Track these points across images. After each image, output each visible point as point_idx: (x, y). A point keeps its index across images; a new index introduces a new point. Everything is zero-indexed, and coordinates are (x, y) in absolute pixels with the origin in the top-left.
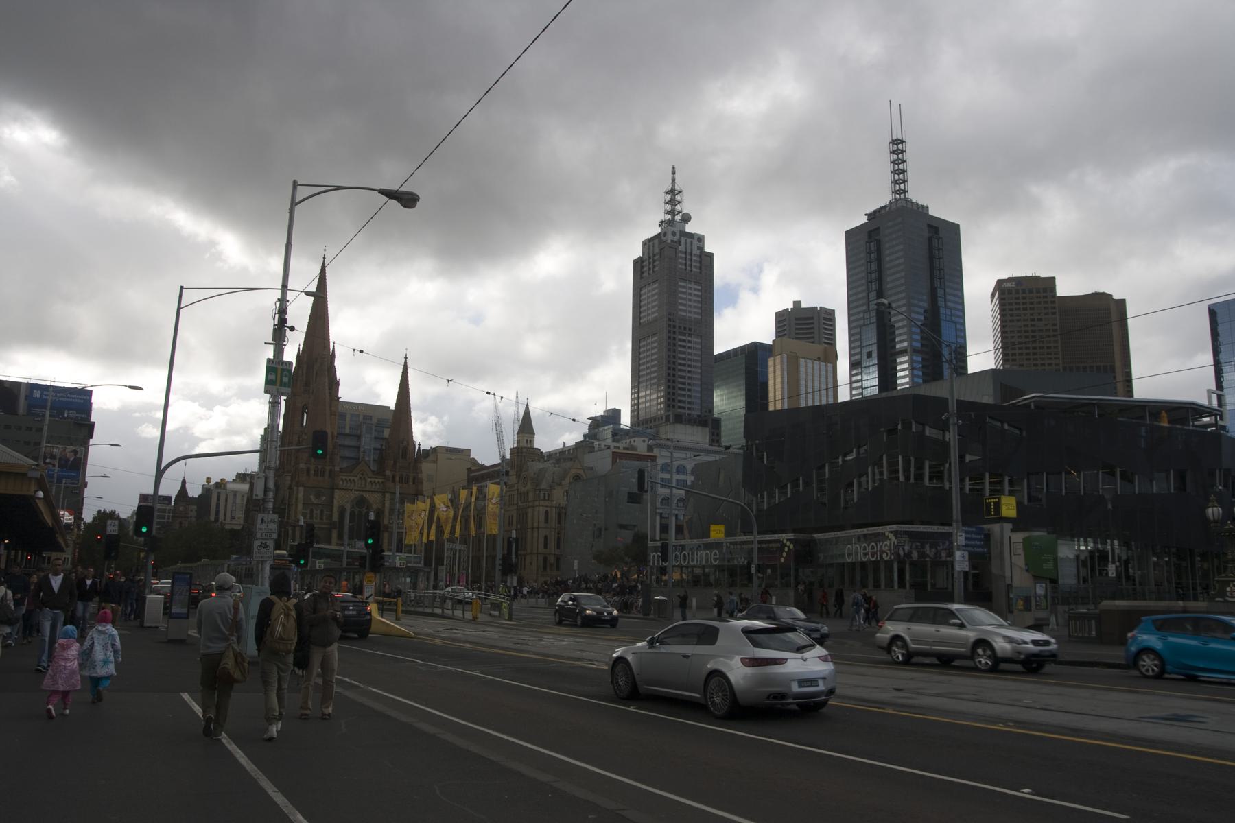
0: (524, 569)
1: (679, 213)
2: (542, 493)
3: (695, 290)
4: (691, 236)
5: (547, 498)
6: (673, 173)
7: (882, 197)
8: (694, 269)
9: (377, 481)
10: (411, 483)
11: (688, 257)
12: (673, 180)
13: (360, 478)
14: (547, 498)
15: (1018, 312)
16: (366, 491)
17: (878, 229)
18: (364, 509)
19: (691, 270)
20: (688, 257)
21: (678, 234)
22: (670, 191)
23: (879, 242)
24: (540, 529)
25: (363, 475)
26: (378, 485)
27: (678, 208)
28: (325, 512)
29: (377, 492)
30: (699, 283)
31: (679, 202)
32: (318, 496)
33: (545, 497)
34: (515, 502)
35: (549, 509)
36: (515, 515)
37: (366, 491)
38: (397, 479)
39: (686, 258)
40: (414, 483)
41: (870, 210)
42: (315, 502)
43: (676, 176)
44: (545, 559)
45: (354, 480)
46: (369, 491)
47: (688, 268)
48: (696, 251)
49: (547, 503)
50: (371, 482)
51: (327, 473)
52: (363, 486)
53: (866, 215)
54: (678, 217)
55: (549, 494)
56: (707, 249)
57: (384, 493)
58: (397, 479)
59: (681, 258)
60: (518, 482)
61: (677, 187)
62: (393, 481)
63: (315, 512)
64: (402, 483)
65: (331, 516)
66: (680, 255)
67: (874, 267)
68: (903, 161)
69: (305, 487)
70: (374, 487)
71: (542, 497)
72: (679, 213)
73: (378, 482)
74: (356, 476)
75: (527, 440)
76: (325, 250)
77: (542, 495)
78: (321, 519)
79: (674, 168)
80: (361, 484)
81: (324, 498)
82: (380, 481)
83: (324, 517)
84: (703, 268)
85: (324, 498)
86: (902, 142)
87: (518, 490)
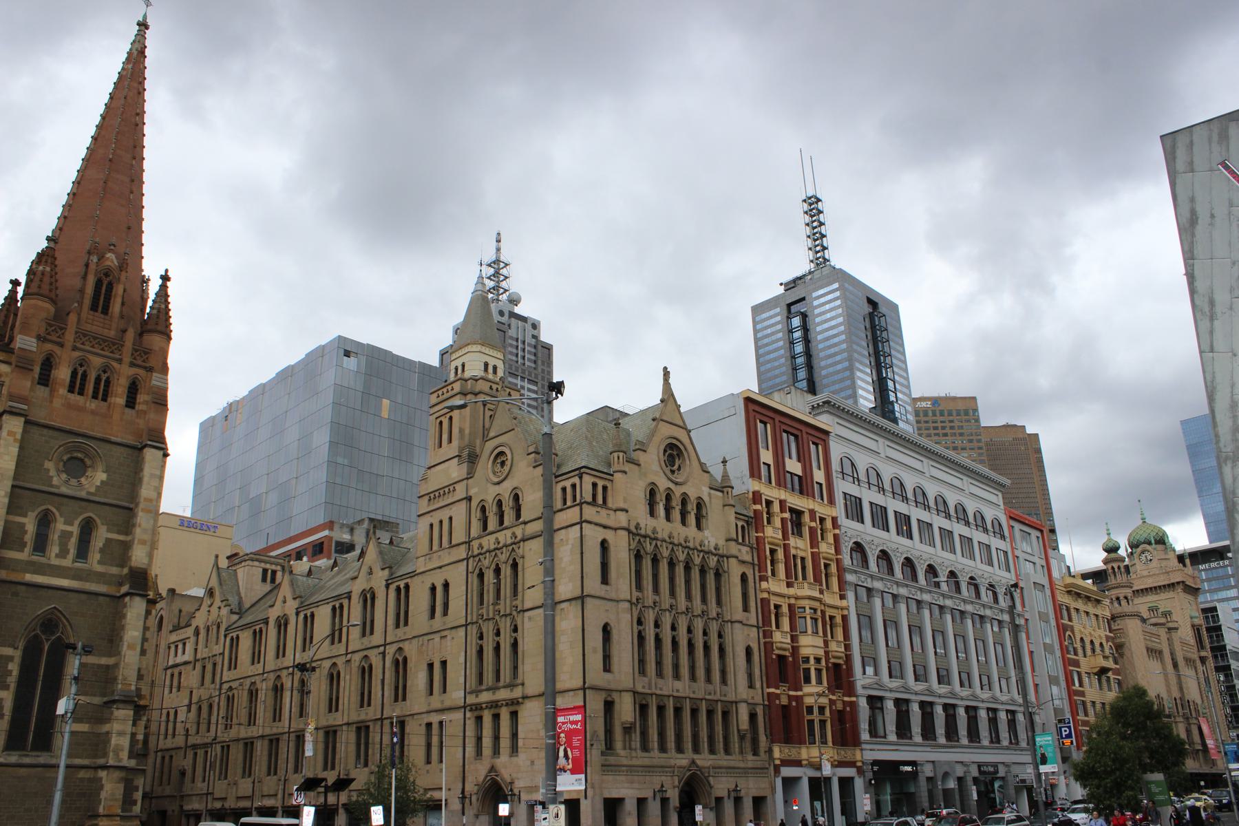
0: (514, 749)
1: (506, 291)
2: (588, 480)
3: (529, 390)
4: (524, 319)
5: (600, 500)
6: (498, 241)
7: (801, 264)
8: (527, 363)
10: (119, 399)
11: (520, 346)
12: (498, 250)
14: (600, 500)
15: (936, 438)
17: (803, 299)
19: (524, 364)
20: (520, 346)
21: (507, 314)
22: (494, 262)
23: (804, 316)
24: (588, 600)
27: (504, 284)
30: (536, 383)
31: (506, 278)
33: (594, 496)
34: (459, 536)
35: (609, 535)
36: (457, 577)
38: (63, 374)
39: (517, 347)
40: (131, 403)
41: (784, 280)
43: (502, 244)
44: (609, 706)
47: (520, 361)
48: (529, 340)
49: (603, 516)
53: (781, 284)
54: (504, 297)
55: (605, 488)
56: (545, 337)
58: (63, 374)
59: (511, 345)
60: (470, 475)
61: (502, 258)
64: (81, 393)
66: (510, 341)
67: (799, 348)
68: (821, 224)
71: (588, 497)
72: (506, 291)
75: (486, 365)
77: (588, 488)
79: (499, 234)
84: (539, 362)
86: (819, 200)
87: (469, 499)
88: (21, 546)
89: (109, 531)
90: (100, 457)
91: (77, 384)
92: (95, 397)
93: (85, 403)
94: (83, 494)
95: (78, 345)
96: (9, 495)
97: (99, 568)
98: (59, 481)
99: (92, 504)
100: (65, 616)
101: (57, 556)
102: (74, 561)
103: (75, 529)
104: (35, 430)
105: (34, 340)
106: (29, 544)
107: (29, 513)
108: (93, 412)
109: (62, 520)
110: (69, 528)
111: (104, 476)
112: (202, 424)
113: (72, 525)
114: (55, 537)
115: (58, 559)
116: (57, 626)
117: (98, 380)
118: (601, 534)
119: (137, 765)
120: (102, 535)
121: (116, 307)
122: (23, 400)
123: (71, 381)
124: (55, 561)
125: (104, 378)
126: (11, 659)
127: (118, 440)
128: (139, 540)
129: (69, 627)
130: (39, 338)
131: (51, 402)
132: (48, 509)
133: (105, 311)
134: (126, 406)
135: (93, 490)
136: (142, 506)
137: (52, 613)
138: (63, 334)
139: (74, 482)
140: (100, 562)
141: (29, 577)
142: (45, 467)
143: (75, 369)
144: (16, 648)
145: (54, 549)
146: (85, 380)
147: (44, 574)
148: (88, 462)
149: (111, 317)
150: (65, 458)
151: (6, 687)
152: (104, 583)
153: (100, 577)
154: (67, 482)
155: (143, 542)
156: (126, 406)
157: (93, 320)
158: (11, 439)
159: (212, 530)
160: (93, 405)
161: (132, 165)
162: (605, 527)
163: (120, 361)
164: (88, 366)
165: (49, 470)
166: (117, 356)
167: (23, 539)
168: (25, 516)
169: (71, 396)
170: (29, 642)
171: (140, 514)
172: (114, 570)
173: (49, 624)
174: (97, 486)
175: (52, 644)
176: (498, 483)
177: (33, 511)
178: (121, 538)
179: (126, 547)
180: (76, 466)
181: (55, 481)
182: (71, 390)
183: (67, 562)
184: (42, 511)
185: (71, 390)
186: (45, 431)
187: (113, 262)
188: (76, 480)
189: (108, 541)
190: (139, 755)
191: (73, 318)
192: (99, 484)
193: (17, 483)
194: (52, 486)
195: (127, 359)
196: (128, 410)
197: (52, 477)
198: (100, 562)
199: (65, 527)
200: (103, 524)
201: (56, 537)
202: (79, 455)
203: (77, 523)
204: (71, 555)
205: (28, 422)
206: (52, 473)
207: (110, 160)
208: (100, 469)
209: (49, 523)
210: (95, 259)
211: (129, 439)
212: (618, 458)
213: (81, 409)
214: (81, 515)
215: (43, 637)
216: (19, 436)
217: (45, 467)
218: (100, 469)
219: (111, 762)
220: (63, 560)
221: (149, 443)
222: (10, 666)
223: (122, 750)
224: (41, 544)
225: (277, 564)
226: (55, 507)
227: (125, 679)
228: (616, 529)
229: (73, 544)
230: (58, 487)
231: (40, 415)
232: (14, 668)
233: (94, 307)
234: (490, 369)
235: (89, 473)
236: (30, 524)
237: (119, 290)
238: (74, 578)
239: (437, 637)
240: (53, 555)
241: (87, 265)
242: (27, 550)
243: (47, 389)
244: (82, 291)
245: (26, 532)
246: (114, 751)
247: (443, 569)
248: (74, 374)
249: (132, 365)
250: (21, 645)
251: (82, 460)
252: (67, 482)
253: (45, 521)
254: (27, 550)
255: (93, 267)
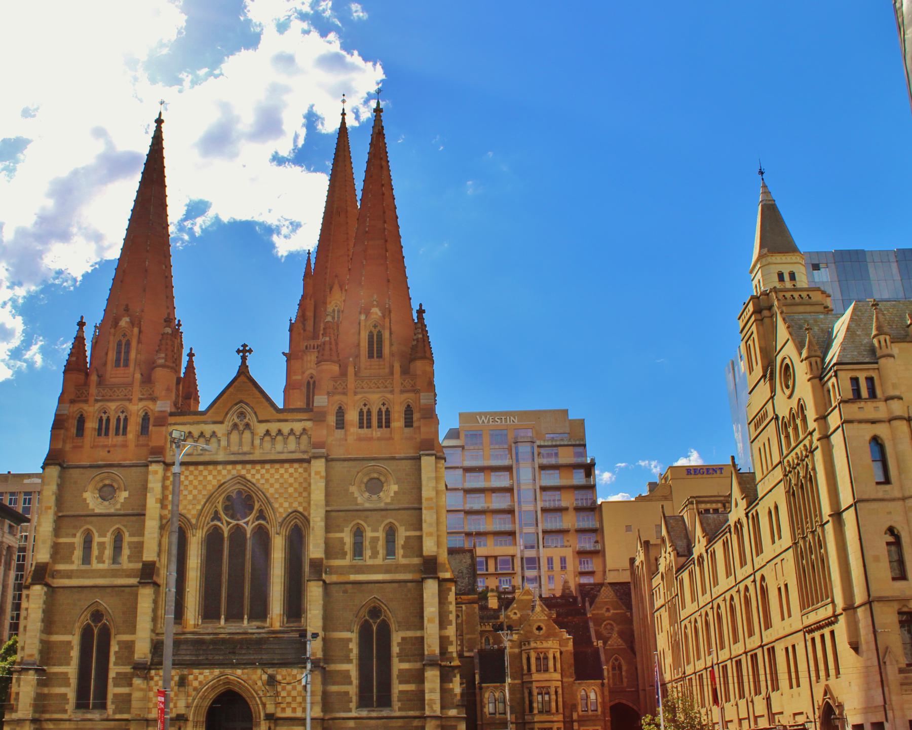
9: (286, 428)
10: (398, 423)
13: (235, 426)
16: (253, 462)
18: (250, 518)
25: (242, 415)
26: (292, 438)
28: (127, 538)
29: (291, 461)
32: (107, 492)
34: (776, 459)
37: (253, 462)
38: (352, 416)
40: (409, 423)
42: (97, 511)
45: (214, 434)
46: (263, 462)
50: (268, 433)
51: (133, 427)
52: (246, 448)
57: (308, 461)
58: (352, 416)
62: (341, 424)
63: (97, 539)
64: (369, 426)
65: (138, 548)
69: (63, 468)
70: (279, 446)
73: (292, 432)
74: (222, 423)
76: (344, 101)
78: (115, 559)
80: (241, 444)
81: (125, 494)
82: (298, 427)
83: (126, 552)
85: (125, 494)
87: (777, 418)
88: (344, 555)
89: (406, 530)
90: (390, 474)
91: (365, 421)
92: (380, 426)
93: (372, 434)
94: (382, 505)
95: (359, 390)
96: (324, 518)
97: (403, 561)
98: (362, 499)
99: (389, 512)
100: (383, 603)
101: (370, 557)
102: (385, 559)
103: (381, 534)
104: (338, 466)
105: (326, 397)
106: (349, 552)
107: (345, 529)
108: (379, 439)
109: (370, 528)
110: (375, 534)
111: (395, 488)
112: (450, 429)
113: (378, 531)
114: (367, 543)
115: (371, 560)
116: (380, 611)
117: (380, 411)
118: (869, 431)
119: (458, 714)
120: (402, 534)
121: (386, 350)
122: (321, 445)
123: (359, 419)
124: (370, 562)
125: (384, 409)
126: (350, 640)
127: (402, 455)
128: (426, 534)
129: (388, 611)
130: (328, 393)
131: (346, 440)
132: (358, 523)
133: (380, 355)
134: (406, 426)
135: (389, 500)
136: (425, 504)
137: (375, 602)
138: (346, 385)
139: (375, 497)
140: (403, 556)
141: (353, 577)
142: (350, 491)
143: (361, 409)
144: (352, 632)
145: (368, 553)
146: (370, 415)
147: (363, 573)
148: (383, 479)
149: (384, 359)
150: (365, 480)
151: (349, 661)
152: (409, 572)
153: (405, 568)
154: (368, 500)
155: (431, 534)
156: (406, 426)
157: (371, 365)
158: (318, 477)
159: (718, 472)
160: (376, 433)
161: (385, 229)
162: (873, 422)
163: (392, 392)
164: (370, 404)
165: (353, 493)
166: (390, 389)
167: (343, 549)
168: (342, 531)
169: (361, 431)
170: (362, 626)
171: (424, 511)
172: (416, 561)
173: (375, 612)
174: (391, 497)
175: (378, 627)
176: (790, 397)
177: (347, 527)
178: (417, 533)
179: (420, 538)
180: (375, 486)
181: (360, 500)
182: (361, 427)
183: (379, 561)
184: (354, 526)
185: (361, 427)
186: (346, 464)
187: (376, 314)
188: (376, 496)
189: (407, 538)
190: (458, 705)
191: (351, 370)
192: (392, 494)
193: (328, 509)
194: (357, 504)
195: (397, 390)
196: (407, 430)
197: (356, 498)
198: (403, 556)
199: (374, 534)
200: (401, 526)
201: (367, 543)
202: (375, 475)
203: (381, 529)
204: (381, 556)
205: (328, 460)
206: (356, 494)
207: (367, 232)
208: (392, 482)
209: (362, 533)
210: (363, 317)
211: (411, 453)
212: (885, 340)
213: (370, 439)
214: (383, 522)
215: (371, 621)
216: (323, 474)
217: (350, 491)
218: (392, 482)
219: (427, 713)
220: (375, 560)
221: (422, 452)
222: (351, 646)
223: (435, 704)
224: (358, 550)
225: (717, 502)
226: (363, 520)
227: (429, 646)
228: (890, 421)
229: (381, 545)
230: (362, 504)
231: (338, 453)
232: (354, 647)
233: (371, 356)
234: (787, 277)
235: (385, 488)
236: (347, 537)
237: (386, 335)
238: (387, 571)
239: (778, 560)
240: (368, 557)
241: (359, 324)
242: (348, 557)
243: (343, 431)
244: (358, 345)
245: (345, 544)
246: (428, 705)
247: (773, 491)
248: (361, 413)
249: (402, 392)
250: (356, 628)
251: (378, 479)
252: (368, 500)
253: (358, 533)
254: (349, 556)
255: (362, 324)
